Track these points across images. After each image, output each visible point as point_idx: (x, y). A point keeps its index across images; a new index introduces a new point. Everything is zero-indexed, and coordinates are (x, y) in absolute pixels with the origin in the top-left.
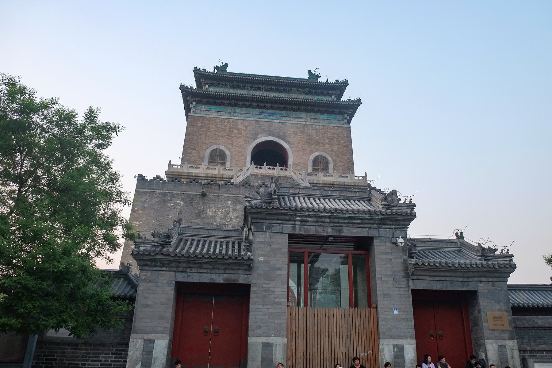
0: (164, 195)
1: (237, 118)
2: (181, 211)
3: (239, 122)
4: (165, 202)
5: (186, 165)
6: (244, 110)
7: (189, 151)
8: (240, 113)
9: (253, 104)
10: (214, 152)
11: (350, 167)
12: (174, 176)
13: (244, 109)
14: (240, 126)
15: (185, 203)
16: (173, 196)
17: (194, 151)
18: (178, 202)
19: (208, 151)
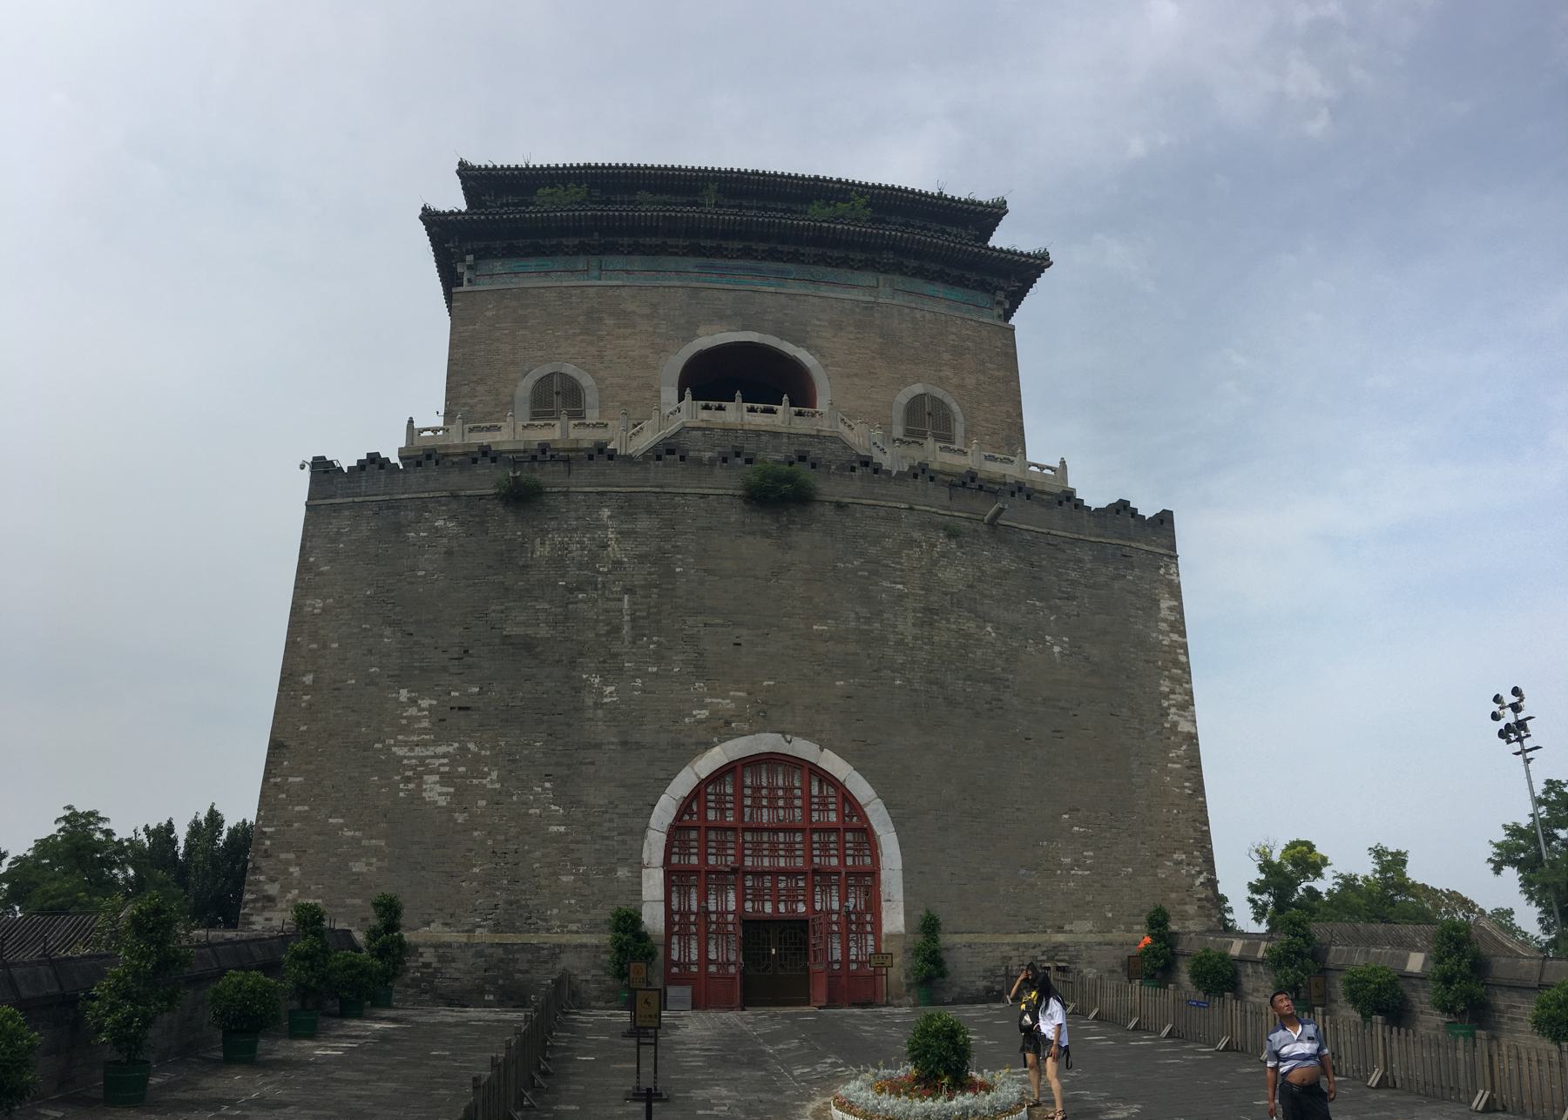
0: (393, 505)
1: (619, 283)
2: (449, 553)
3: (625, 293)
4: (399, 529)
5: (455, 428)
6: (637, 262)
7: (465, 390)
8: (627, 272)
9: (670, 241)
10: (546, 381)
11: (1014, 437)
12: (423, 456)
13: (636, 258)
14: (630, 307)
15: (461, 524)
16: (423, 506)
17: (481, 389)
18: (439, 523)
19: (524, 387)
